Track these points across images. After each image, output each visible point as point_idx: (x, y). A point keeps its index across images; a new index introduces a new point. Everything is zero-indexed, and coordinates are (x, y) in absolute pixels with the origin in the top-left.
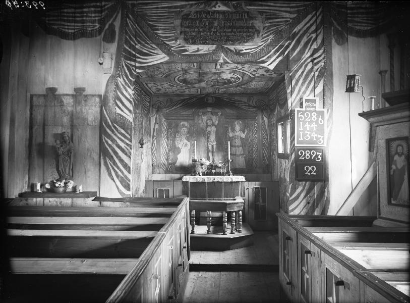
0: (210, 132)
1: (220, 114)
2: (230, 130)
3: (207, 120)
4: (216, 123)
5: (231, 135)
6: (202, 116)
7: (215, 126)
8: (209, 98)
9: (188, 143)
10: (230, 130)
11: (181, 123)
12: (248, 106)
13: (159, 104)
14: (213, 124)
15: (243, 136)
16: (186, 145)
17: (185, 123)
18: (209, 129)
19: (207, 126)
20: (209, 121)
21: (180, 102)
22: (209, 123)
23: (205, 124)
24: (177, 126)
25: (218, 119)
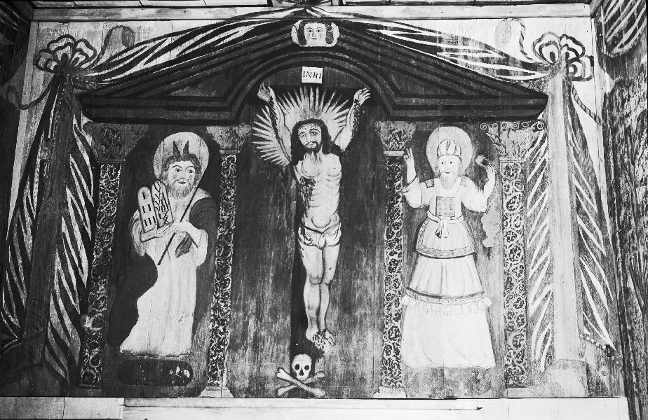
0: (309, 182)
1: (361, 97)
2: (411, 172)
3: (299, 125)
4: (344, 141)
5: (415, 193)
6: (276, 105)
7: (335, 150)
8: (315, 26)
9: (200, 236)
10: (411, 172)
11: (168, 141)
12: (499, 62)
13: (68, 50)
14: (328, 145)
15: (477, 199)
16: (186, 245)
17: (190, 140)
18: (306, 167)
19: (299, 151)
20: (306, 129)
21: (169, 41)
22: (309, 138)
23: (288, 143)
24: (147, 148)
25: (351, 119)
